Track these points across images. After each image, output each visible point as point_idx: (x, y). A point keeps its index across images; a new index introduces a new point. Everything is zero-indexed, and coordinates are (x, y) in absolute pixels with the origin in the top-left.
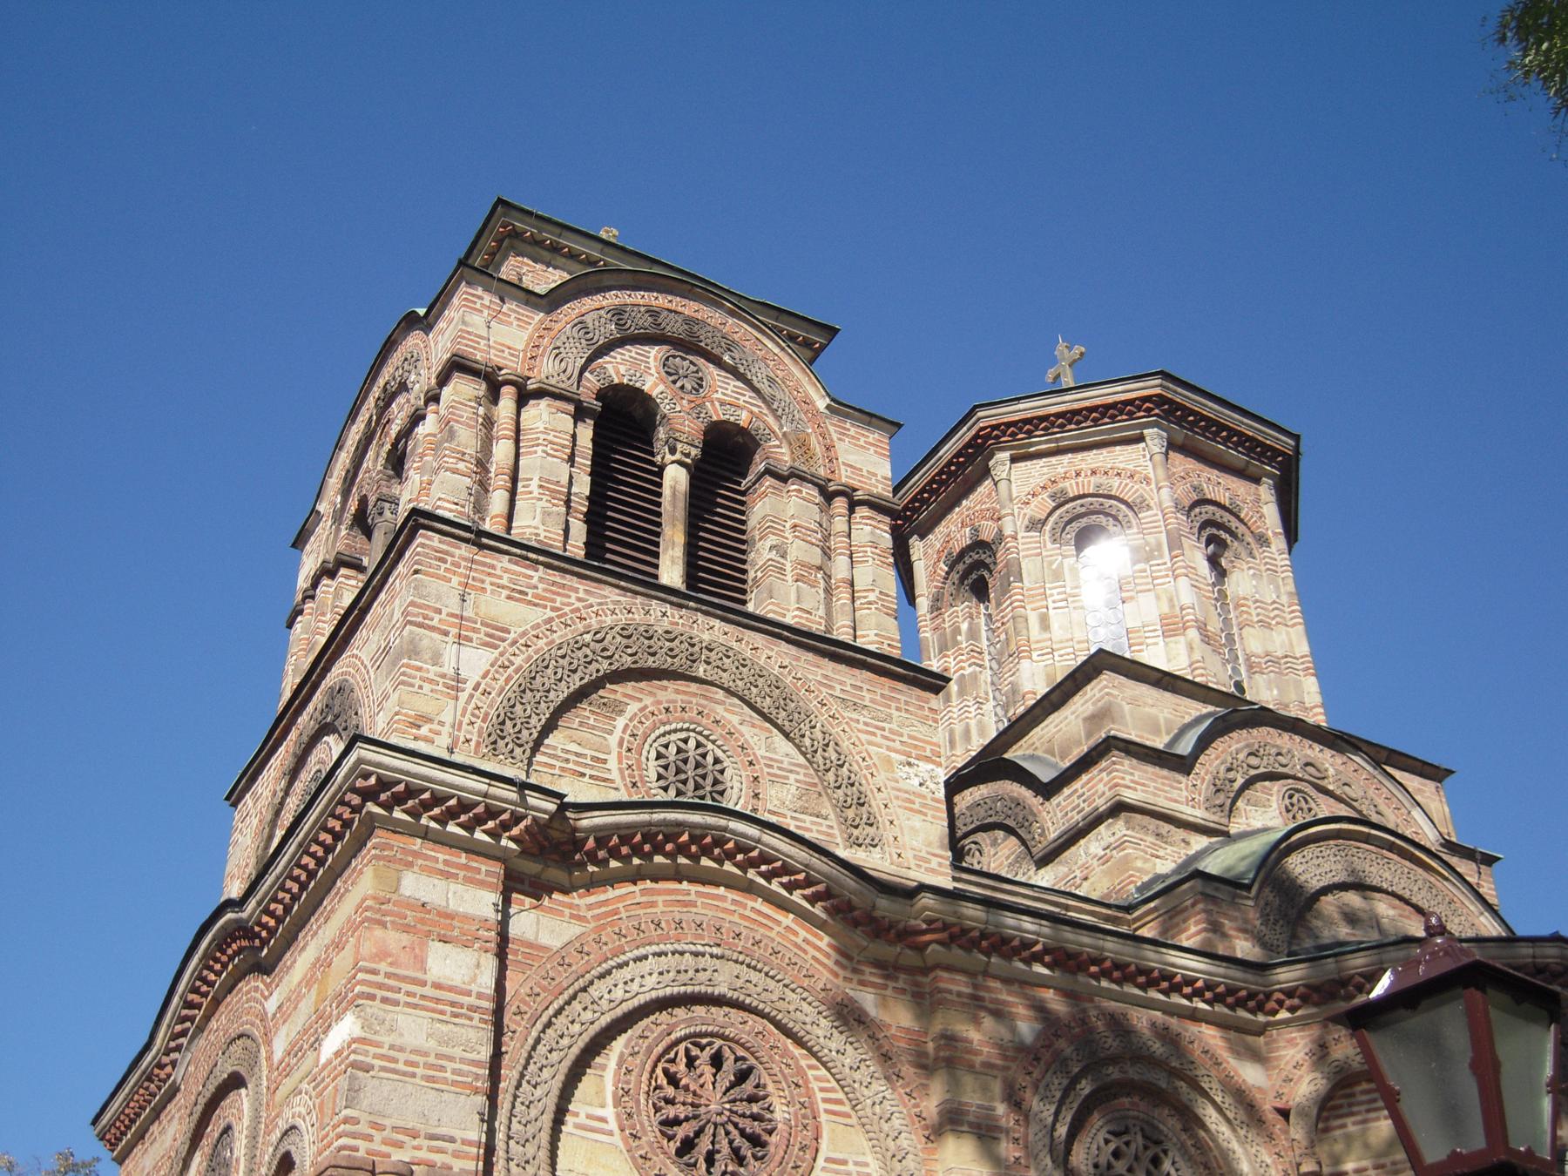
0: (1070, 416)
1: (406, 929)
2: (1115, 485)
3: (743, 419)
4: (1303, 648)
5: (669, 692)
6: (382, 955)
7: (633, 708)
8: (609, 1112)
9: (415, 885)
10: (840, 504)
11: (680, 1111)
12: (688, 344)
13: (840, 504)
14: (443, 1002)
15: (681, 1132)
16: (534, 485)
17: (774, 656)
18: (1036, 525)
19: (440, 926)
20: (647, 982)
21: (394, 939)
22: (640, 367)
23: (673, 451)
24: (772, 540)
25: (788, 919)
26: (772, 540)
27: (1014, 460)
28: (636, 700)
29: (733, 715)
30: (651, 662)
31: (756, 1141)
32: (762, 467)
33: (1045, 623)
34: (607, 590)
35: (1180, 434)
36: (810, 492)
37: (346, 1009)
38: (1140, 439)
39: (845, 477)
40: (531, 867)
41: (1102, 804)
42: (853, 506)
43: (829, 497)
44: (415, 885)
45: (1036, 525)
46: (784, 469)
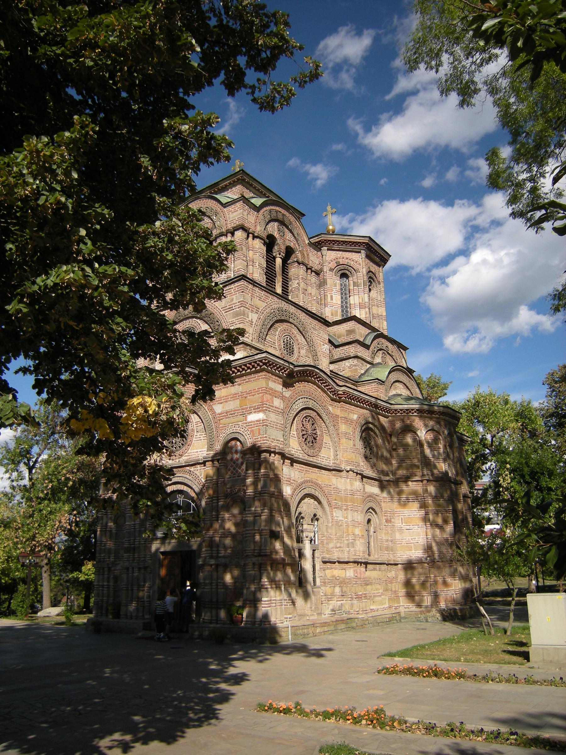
0: (344, 242)
1: (270, 394)
2: (352, 263)
3: (292, 245)
4: (384, 314)
5: (285, 325)
6: (267, 401)
7: (279, 329)
8: (295, 433)
9: (272, 385)
10: (309, 271)
11: (304, 433)
12: (282, 223)
13: (309, 271)
14: (276, 411)
15: (305, 437)
16: (257, 264)
17: (302, 316)
18: (331, 270)
19: (274, 394)
20: (299, 405)
21: (269, 397)
22: (273, 229)
23: (280, 254)
24: (297, 281)
25: (320, 390)
26: (297, 281)
27: (328, 250)
28: (280, 327)
29: (295, 331)
30: (283, 318)
31: (315, 439)
32: (295, 259)
33: (332, 297)
34: (275, 298)
35: (368, 253)
36: (305, 268)
37: (260, 411)
38: (360, 252)
39: (311, 264)
40: (288, 381)
41: (352, 355)
42: (312, 271)
43: (307, 269)
44: (272, 385)
45: (331, 270)
46: (300, 260)
